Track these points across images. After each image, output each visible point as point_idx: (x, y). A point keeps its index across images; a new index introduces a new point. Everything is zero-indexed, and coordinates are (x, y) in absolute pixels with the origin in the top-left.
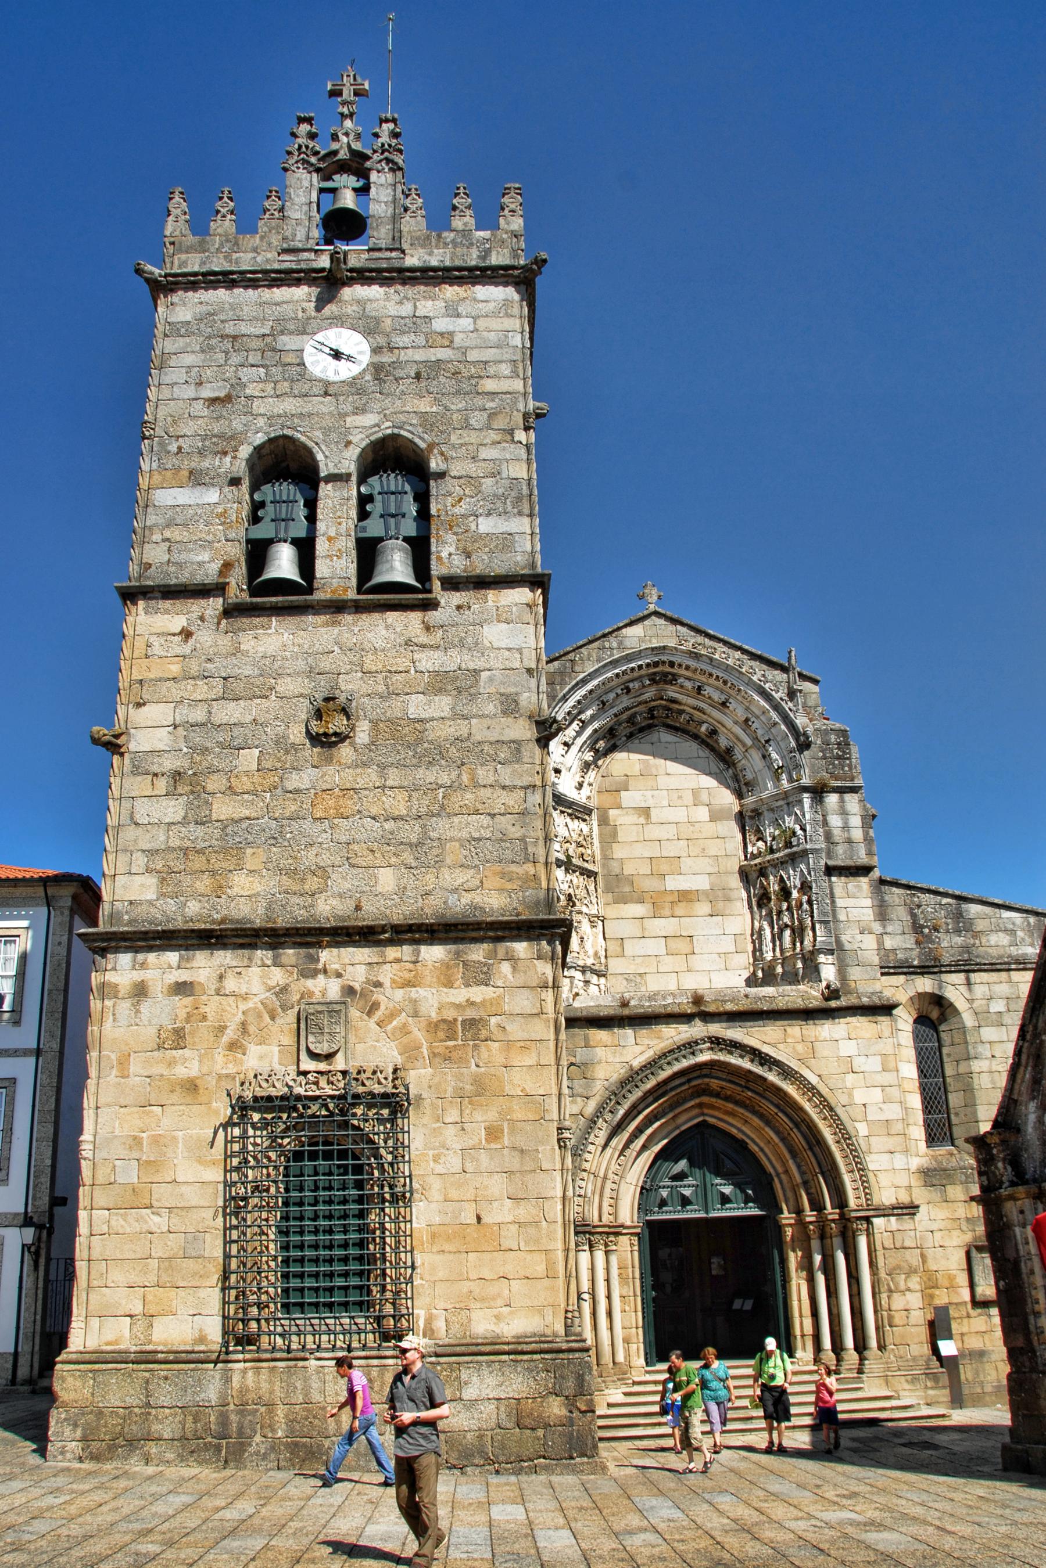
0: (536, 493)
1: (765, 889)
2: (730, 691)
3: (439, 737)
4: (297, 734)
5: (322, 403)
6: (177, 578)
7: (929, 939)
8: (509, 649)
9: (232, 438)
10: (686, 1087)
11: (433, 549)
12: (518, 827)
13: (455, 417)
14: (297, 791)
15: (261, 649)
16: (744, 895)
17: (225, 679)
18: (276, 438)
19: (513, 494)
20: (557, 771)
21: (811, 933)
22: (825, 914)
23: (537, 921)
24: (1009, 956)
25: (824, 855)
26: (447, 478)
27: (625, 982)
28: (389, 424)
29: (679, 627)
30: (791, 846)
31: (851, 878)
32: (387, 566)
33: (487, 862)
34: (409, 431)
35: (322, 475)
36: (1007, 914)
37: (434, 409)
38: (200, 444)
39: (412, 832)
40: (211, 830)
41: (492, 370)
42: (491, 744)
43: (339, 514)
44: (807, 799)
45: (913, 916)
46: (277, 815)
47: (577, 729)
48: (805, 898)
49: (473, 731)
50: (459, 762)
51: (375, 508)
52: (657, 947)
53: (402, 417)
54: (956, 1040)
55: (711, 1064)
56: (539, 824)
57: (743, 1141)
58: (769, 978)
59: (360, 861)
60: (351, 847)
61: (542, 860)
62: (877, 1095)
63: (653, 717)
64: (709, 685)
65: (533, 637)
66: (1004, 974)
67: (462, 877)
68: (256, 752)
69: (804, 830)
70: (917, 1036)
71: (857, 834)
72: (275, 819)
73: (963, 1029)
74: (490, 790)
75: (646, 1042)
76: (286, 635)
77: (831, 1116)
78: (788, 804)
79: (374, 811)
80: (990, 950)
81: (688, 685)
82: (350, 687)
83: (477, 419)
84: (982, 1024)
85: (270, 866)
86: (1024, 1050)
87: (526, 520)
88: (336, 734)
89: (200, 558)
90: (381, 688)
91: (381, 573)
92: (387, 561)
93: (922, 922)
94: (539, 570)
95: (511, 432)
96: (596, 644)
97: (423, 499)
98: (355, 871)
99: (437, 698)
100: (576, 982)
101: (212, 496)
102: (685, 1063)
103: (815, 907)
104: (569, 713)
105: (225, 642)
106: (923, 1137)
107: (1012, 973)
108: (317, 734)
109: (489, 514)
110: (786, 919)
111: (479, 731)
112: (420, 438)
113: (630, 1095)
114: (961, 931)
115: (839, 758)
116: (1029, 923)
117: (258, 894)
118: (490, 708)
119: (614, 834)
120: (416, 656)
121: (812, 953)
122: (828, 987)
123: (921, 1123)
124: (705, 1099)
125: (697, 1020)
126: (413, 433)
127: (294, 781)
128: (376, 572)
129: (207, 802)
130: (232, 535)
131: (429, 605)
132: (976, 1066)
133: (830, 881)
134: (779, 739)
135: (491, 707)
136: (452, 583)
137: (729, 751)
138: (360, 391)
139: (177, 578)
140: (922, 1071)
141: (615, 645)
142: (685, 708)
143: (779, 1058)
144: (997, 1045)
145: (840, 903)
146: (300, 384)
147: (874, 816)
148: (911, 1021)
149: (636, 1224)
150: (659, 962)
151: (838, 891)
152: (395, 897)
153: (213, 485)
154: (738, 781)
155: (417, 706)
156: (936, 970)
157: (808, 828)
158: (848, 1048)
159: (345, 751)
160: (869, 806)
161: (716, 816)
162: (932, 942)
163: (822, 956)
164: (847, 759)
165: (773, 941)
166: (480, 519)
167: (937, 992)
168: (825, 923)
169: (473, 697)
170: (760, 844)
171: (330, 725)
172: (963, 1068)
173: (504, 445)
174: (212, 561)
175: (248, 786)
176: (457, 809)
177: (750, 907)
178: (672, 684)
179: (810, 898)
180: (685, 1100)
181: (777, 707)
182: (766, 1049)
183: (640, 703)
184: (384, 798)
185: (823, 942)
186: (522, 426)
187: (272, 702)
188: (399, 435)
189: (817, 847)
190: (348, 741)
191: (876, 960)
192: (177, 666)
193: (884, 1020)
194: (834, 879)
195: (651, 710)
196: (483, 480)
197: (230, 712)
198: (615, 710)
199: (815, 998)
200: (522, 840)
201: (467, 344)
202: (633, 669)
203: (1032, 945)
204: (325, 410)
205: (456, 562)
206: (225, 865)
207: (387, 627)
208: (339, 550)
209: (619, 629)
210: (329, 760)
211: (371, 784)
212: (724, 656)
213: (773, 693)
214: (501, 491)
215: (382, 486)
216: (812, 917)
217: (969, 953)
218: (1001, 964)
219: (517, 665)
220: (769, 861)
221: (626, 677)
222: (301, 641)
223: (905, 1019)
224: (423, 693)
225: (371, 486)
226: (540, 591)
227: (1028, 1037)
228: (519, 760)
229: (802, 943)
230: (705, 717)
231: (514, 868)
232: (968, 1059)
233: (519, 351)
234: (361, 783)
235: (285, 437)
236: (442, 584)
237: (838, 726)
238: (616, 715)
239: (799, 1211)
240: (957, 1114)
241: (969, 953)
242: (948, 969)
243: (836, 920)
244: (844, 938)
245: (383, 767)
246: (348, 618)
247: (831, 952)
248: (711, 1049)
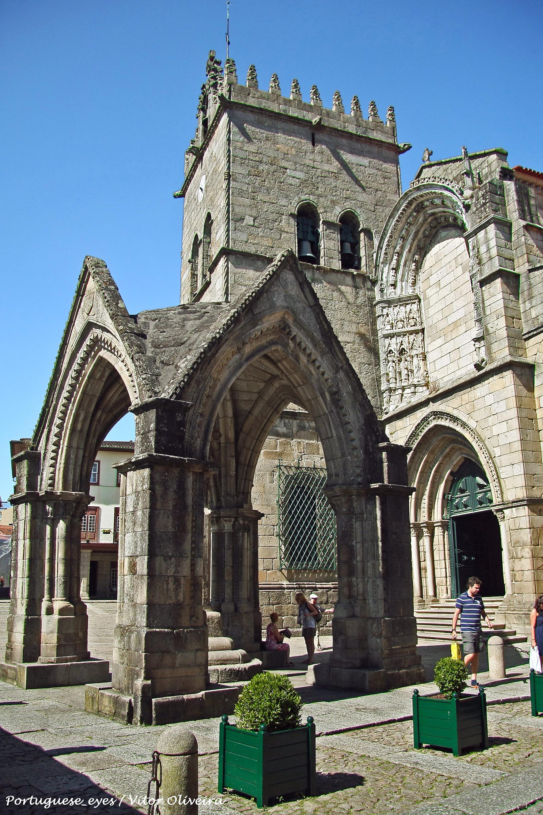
20: (392, 285)
47: (395, 257)
55: (436, 426)
100: (404, 395)
104: (386, 254)
133: (482, 290)
145: (487, 303)
164: (488, 202)
191: (504, 333)
198: (411, 237)
202: (402, 213)
221: (404, 219)
238: (413, 240)
244: (489, 326)
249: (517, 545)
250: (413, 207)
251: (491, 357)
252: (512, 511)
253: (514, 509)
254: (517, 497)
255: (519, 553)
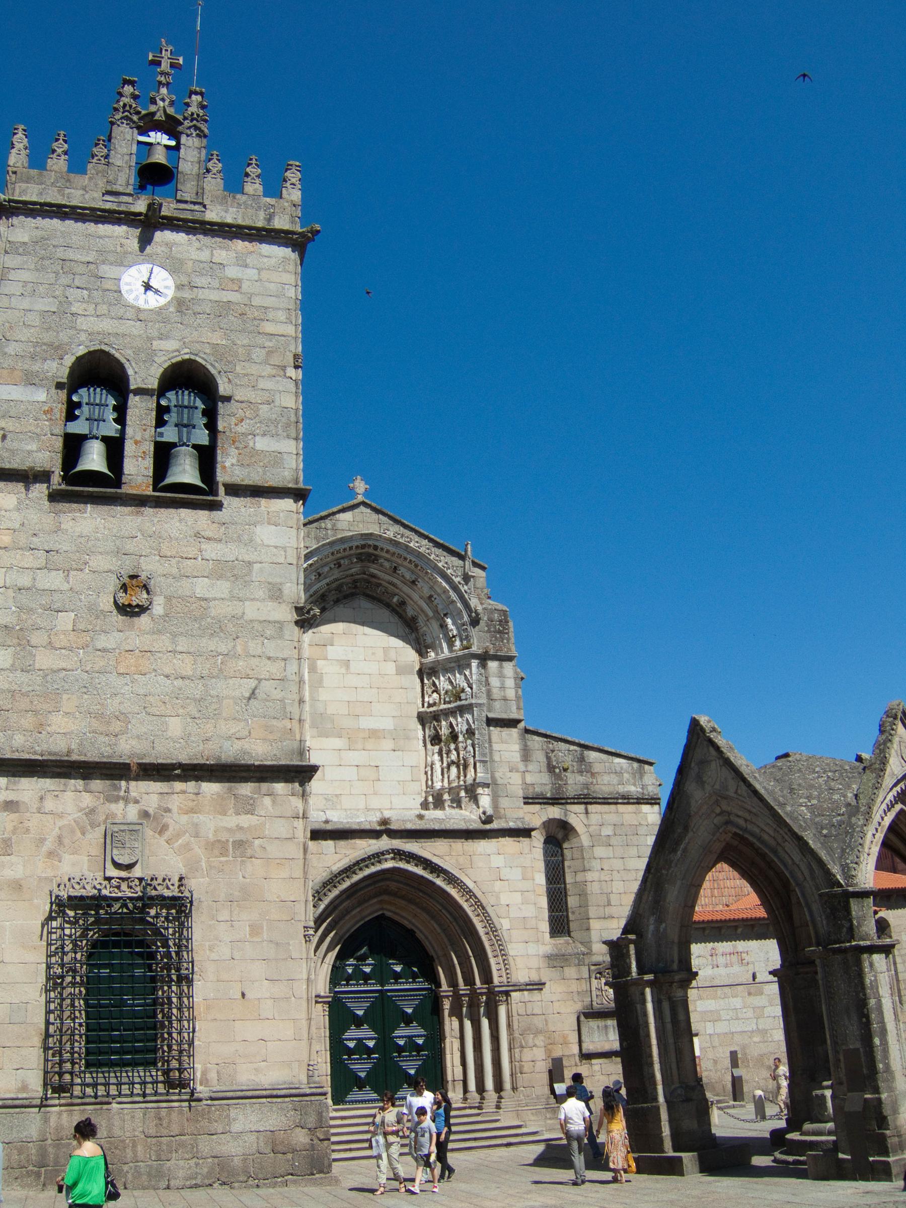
0: (301, 421)
1: (437, 732)
2: (420, 573)
3: (220, 614)
4: (106, 603)
5: (134, 326)
6: (10, 462)
7: (558, 777)
8: (276, 547)
9: (58, 347)
10: (372, 887)
11: (219, 458)
12: (279, 690)
13: (240, 350)
14: (104, 650)
15: (78, 529)
16: (420, 733)
17: (47, 552)
18: (95, 351)
19: (284, 420)
21: (473, 770)
22: (484, 755)
23: (293, 766)
24: (618, 793)
25: (485, 709)
26: (232, 401)
27: (324, 802)
28: (187, 350)
29: (381, 516)
30: (460, 700)
31: (505, 729)
32: (180, 468)
33: (255, 717)
34: (203, 358)
35: (132, 387)
36: (618, 760)
37: (224, 342)
38: (32, 350)
39: (196, 689)
40: (34, 677)
41: (270, 316)
42: (260, 622)
43: (144, 422)
44: (474, 663)
45: (548, 758)
46: (88, 669)
48: (469, 742)
49: (246, 611)
50: (235, 636)
51: (171, 418)
52: (350, 774)
53: (198, 346)
54: (575, 856)
56: (295, 689)
57: (412, 930)
58: (439, 803)
59: (154, 710)
60: (147, 698)
61: (297, 717)
62: (517, 897)
63: (356, 587)
64: (403, 566)
65: (295, 539)
66: (613, 807)
67: (234, 728)
68: (73, 615)
69: (471, 688)
70: (546, 852)
71: (511, 693)
72: (87, 672)
73: (581, 848)
74: (258, 659)
75: (344, 851)
76: (99, 519)
77: (483, 914)
78: (459, 666)
79: (167, 670)
80: (604, 788)
81: (387, 564)
82: (150, 567)
83: (258, 354)
84: (595, 844)
85: (83, 710)
86: (649, 880)
87: (293, 443)
88: (138, 606)
89: (29, 448)
90: (175, 571)
91: (174, 475)
92: (181, 464)
93: (554, 763)
94: (301, 485)
95: (283, 368)
96: (315, 525)
97: (211, 416)
98: (151, 718)
99: (219, 582)
101: (41, 395)
102: (373, 869)
103: (477, 749)
105: (48, 520)
106: (548, 930)
107: (619, 806)
108: (123, 604)
109: (264, 435)
110: (454, 756)
111: (252, 611)
112: (212, 365)
113: (330, 893)
114: (583, 772)
115: (500, 632)
116: (633, 767)
117: (72, 732)
118: (260, 593)
119: (320, 681)
120: (203, 547)
121: (472, 785)
122: (484, 813)
123: (547, 919)
124: (385, 897)
125: (385, 837)
126: (206, 361)
127: (102, 642)
128: (169, 472)
129: (31, 653)
130: (55, 432)
131: (215, 506)
132: (589, 876)
133: (489, 730)
134: (454, 614)
135: (261, 593)
136: (235, 490)
137: (414, 619)
138: (166, 321)
139: (10, 462)
140: (549, 879)
141: (329, 526)
142: (382, 582)
143: (445, 867)
144: (605, 860)
145: (496, 747)
146: (117, 307)
147: (522, 679)
148: (542, 840)
149: (328, 994)
150: (351, 786)
151: (495, 738)
152: (182, 741)
153: (42, 386)
154: (419, 644)
155: (202, 587)
156: (563, 801)
157: (474, 686)
158: (497, 861)
159: (144, 620)
160: (519, 670)
161: (401, 671)
162: (561, 779)
163: (480, 788)
164: (506, 633)
165: (443, 774)
166: (258, 438)
167: (563, 818)
168: (484, 762)
169: (247, 584)
170: (435, 695)
171: (134, 598)
172: (580, 877)
173: (278, 378)
174: (39, 450)
175: (64, 643)
176: (232, 674)
177: (425, 746)
178: (373, 562)
179: (473, 741)
180: (370, 898)
181: (455, 588)
182: (435, 860)
183: (347, 576)
184: (175, 661)
185: (482, 777)
186: (293, 365)
187: (86, 575)
188: (195, 361)
189: (479, 702)
190: (148, 612)
191: (521, 793)
192: (7, 537)
193: (525, 841)
194: (491, 728)
195: (355, 581)
196: (261, 406)
197: (53, 580)
198: (327, 580)
199: (474, 821)
200: (282, 700)
201: (251, 291)
202: (345, 550)
203: (634, 785)
204: (135, 332)
205: (237, 472)
206: (45, 706)
207: (180, 521)
208: (144, 452)
209: (334, 514)
210: (131, 627)
211: (164, 649)
212: (417, 545)
213: (453, 577)
214: (274, 416)
215: (177, 400)
216: (474, 757)
217: (588, 789)
218: (611, 798)
219: (282, 560)
220: (441, 710)
221: (339, 555)
222: (111, 526)
223: (538, 839)
224: (207, 577)
225: (169, 400)
226: (301, 502)
227: (652, 871)
228: (281, 637)
229: (465, 776)
230: (398, 591)
231: (274, 722)
232: (584, 871)
233: (293, 302)
234: (157, 647)
235: (102, 351)
236: (226, 489)
237: (500, 607)
238: (328, 584)
239: (453, 983)
240: (573, 913)
241: (588, 789)
242: (572, 801)
243: (492, 761)
244: (497, 775)
245: (174, 636)
246: (148, 511)
247: (487, 785)
248: (393, 859)
249: (528, 1032)
250: (363, 551)
251: (498, 811)
252: (524, 994)
253: (526, 993)
254: (532, 979)
255: (531, 1041)
